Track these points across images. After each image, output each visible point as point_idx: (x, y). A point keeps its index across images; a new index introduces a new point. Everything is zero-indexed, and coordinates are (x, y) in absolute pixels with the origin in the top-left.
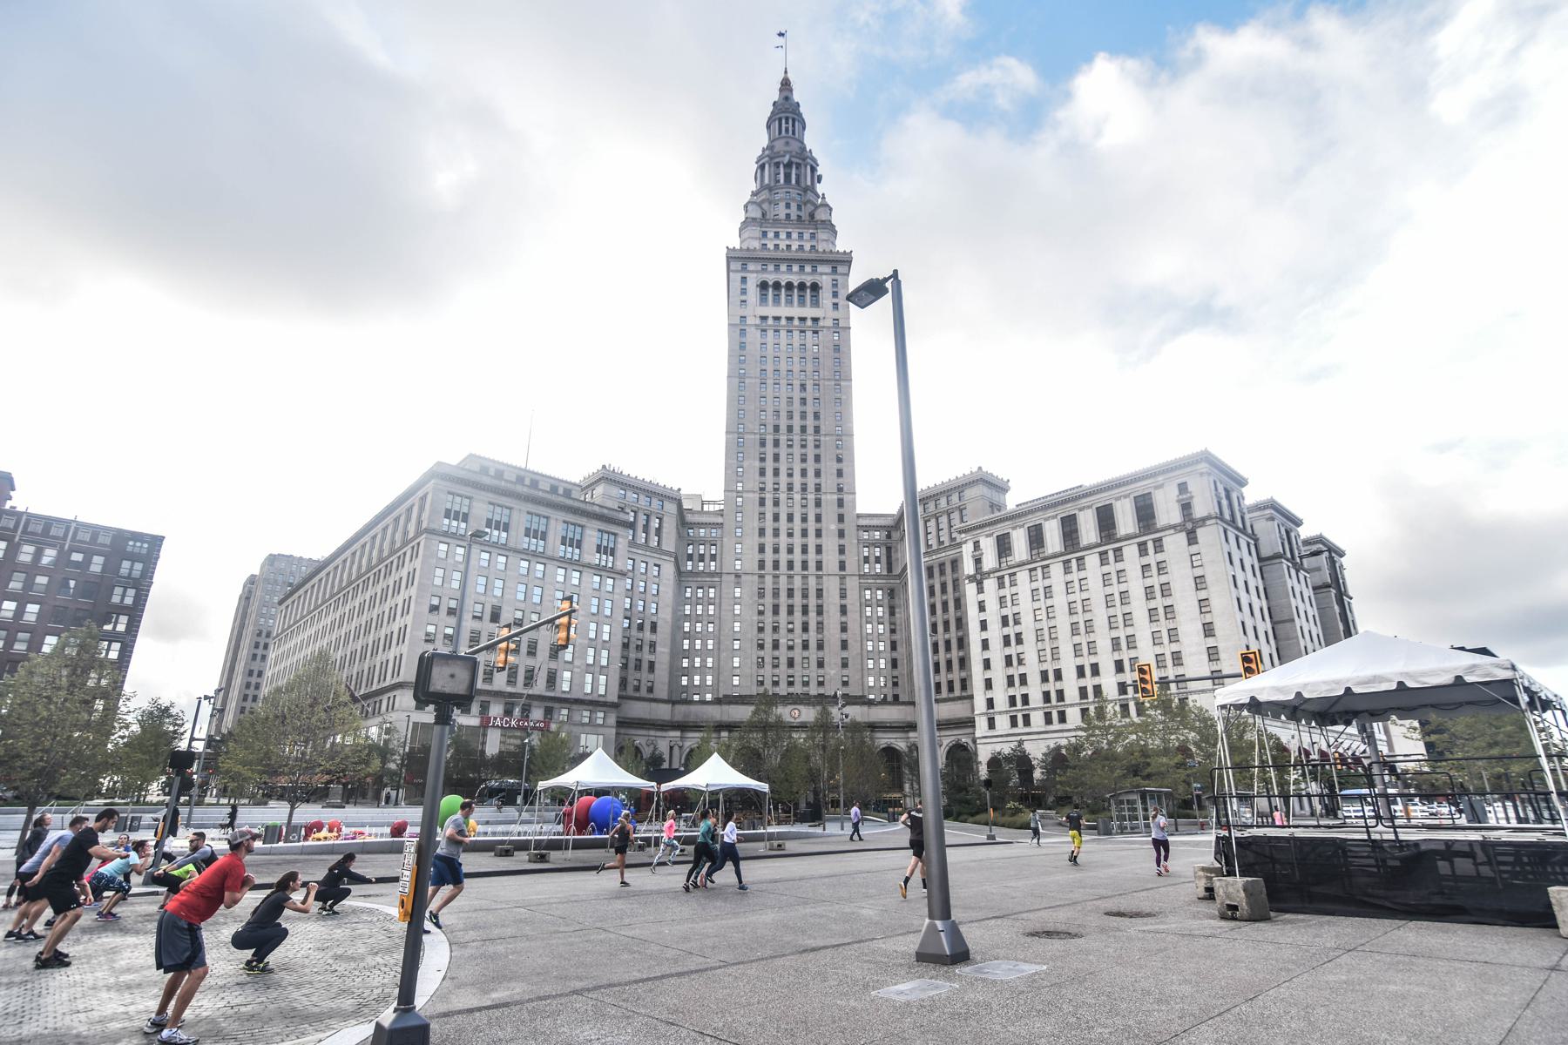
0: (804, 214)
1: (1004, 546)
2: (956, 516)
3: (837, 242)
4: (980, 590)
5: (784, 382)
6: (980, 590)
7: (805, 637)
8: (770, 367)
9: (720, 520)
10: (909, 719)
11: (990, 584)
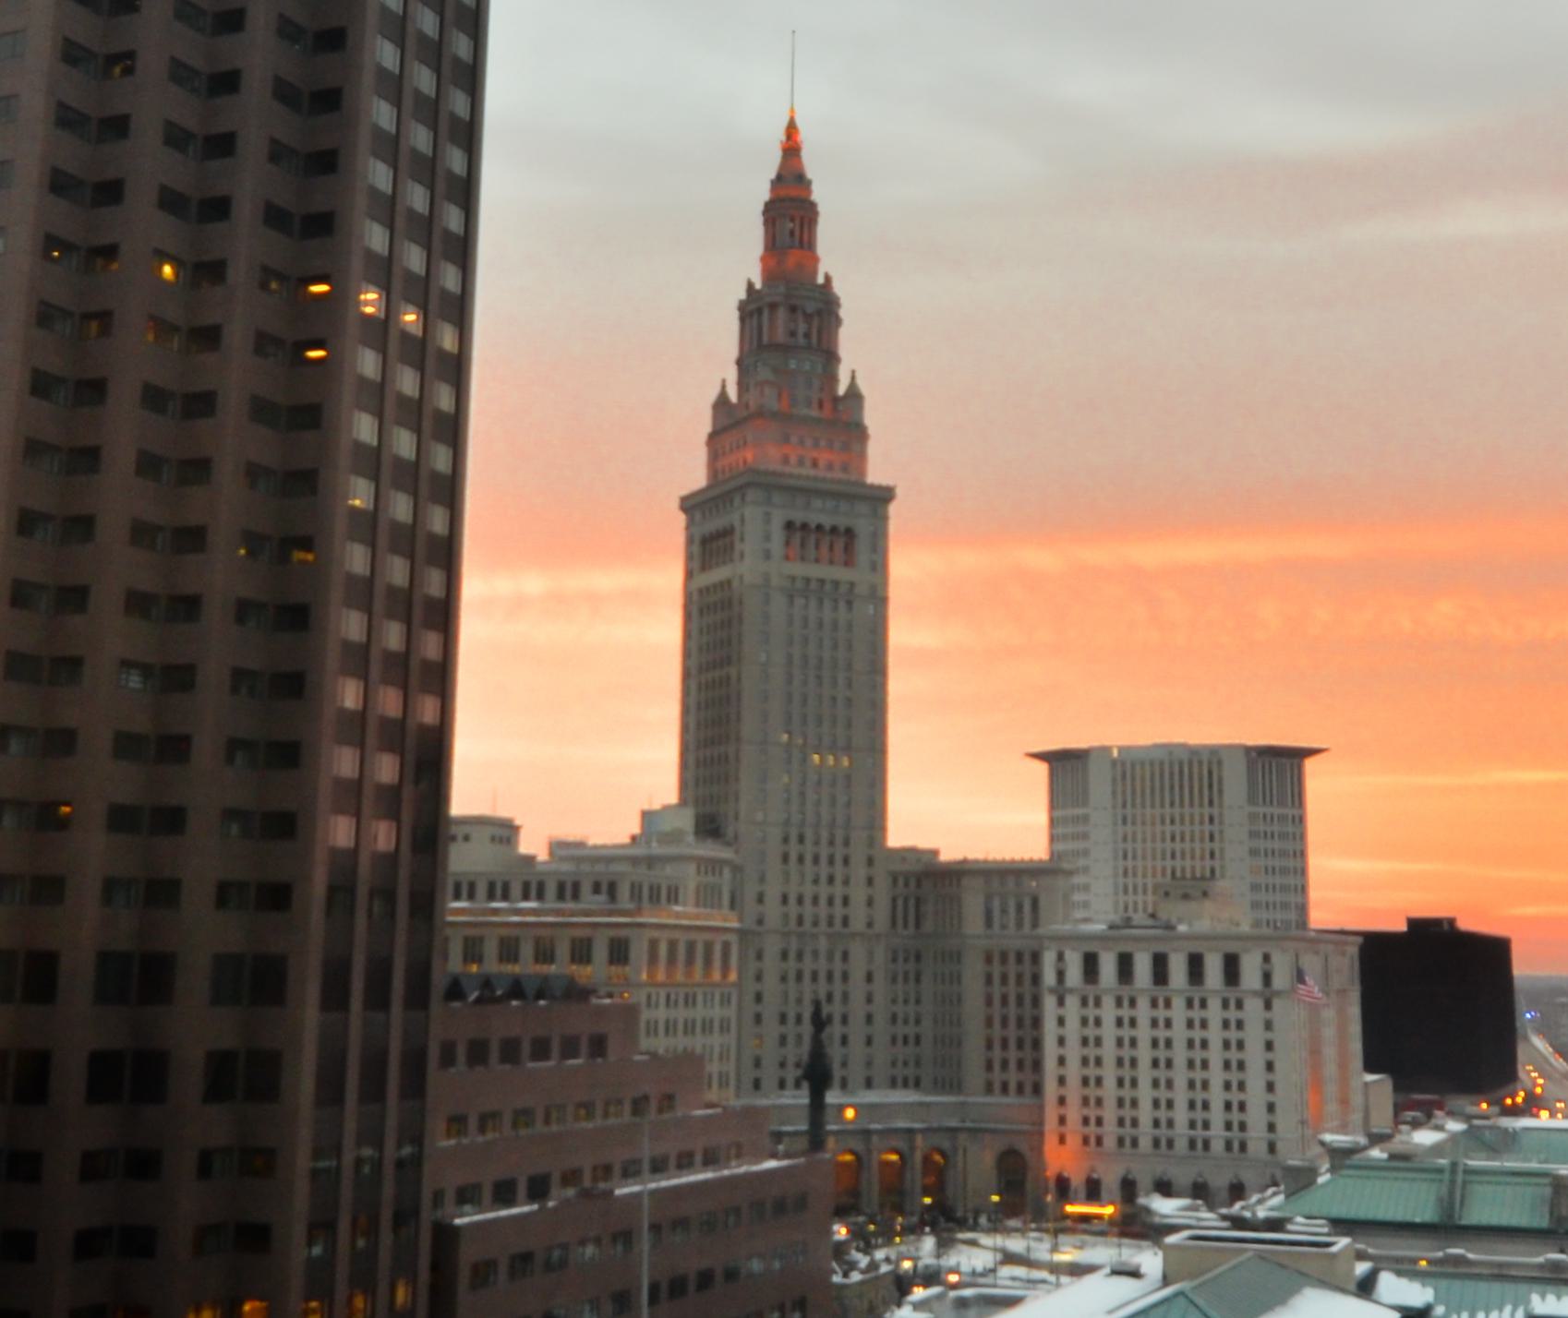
1: (1091, 965)
3: (874, 450)
4: (1061, 1002)
6: (1061, 1002)
11: (1072, 1002)
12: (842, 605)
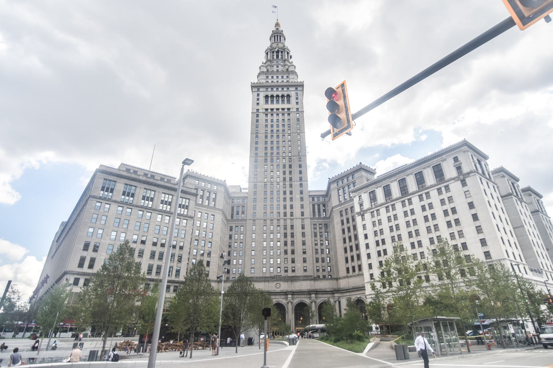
0: (285, 70)
2: (352, 186)
5: (275, 135)
7: (286, 248)
8: (269, 129)
9: (246, 195)
10: (335, 287)
12: (286, 115)
